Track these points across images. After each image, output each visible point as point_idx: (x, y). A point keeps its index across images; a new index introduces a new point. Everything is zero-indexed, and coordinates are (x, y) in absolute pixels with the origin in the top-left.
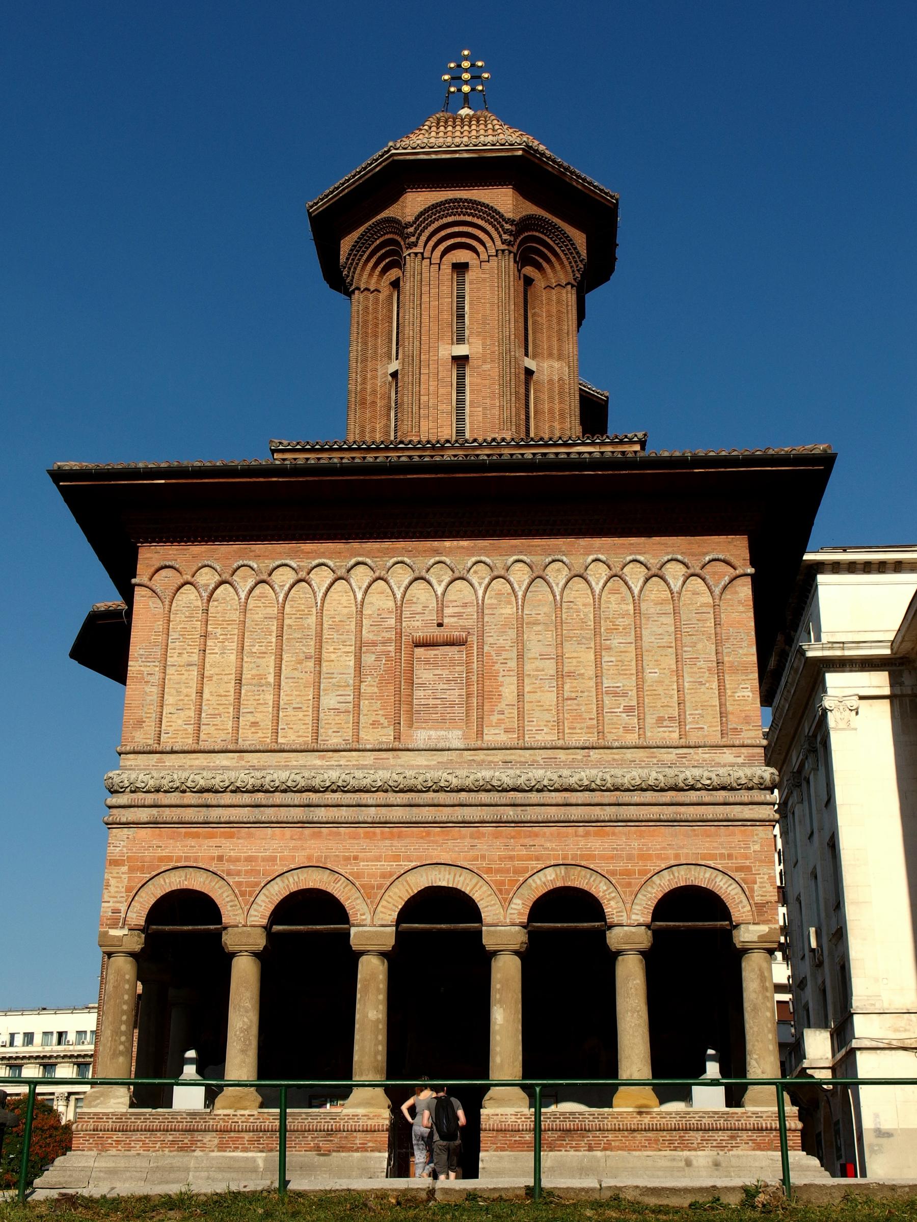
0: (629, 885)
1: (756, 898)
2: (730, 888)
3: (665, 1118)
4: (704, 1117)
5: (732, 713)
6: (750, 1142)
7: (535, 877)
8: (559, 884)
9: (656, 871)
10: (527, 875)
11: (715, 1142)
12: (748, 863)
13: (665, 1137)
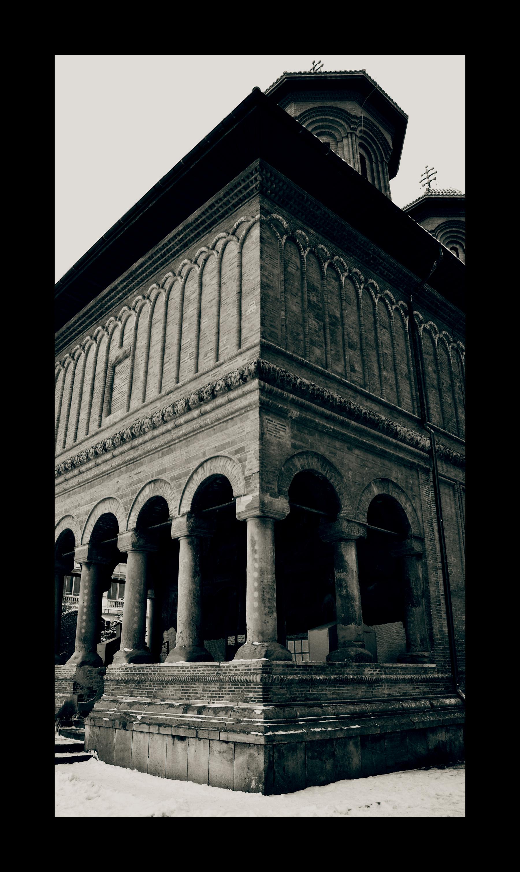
0: (180, 485)
1: (246, 473)
2: (233, 470)
3: (185, 671)
4: (205, 671)
5: (245, 327)
6: (230, 693)
7: (141, 495)
8: (151, 496)
9: (194, 470)
10: (137, 494)
11: (210, 693)
12: (242, 444)
13: (184, 687)
